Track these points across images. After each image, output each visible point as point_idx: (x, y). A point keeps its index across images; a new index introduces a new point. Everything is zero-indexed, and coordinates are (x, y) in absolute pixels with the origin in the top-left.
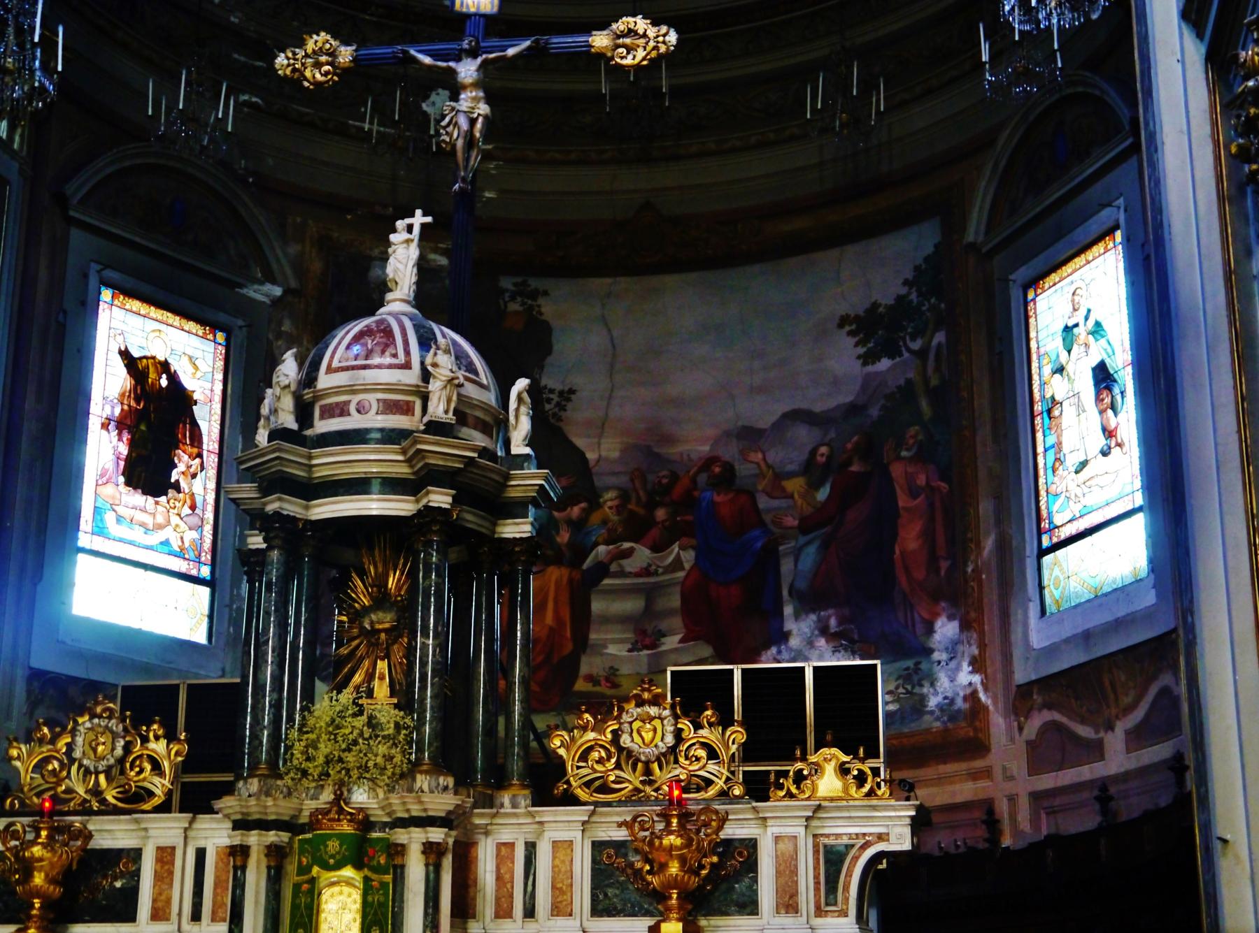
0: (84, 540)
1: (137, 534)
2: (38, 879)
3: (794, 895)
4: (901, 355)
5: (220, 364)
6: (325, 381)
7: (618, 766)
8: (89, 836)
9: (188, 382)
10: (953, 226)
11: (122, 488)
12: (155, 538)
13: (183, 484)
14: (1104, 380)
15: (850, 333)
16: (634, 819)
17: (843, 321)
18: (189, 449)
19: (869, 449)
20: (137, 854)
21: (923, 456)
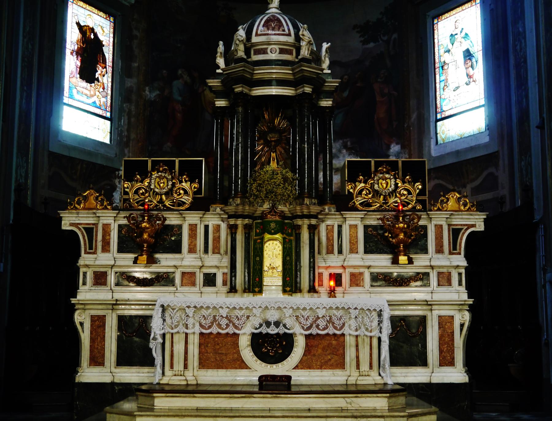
0: (66, 100)
1: (84, 99)
2: (145, 236)
3: (442, 246)
4: (379, 42)
5: (112, 30)
6: (255, 39)
7: (373, 196)
8: (165, 219)
9: (101, 37)
11: (79, 80)
12: (91, 101)
13: (100, 79)
14: (468, 56)
15: (357, 32)
16: (384, 217)
17: (355, 27)
18: (102, 65)
20: (180, 227)
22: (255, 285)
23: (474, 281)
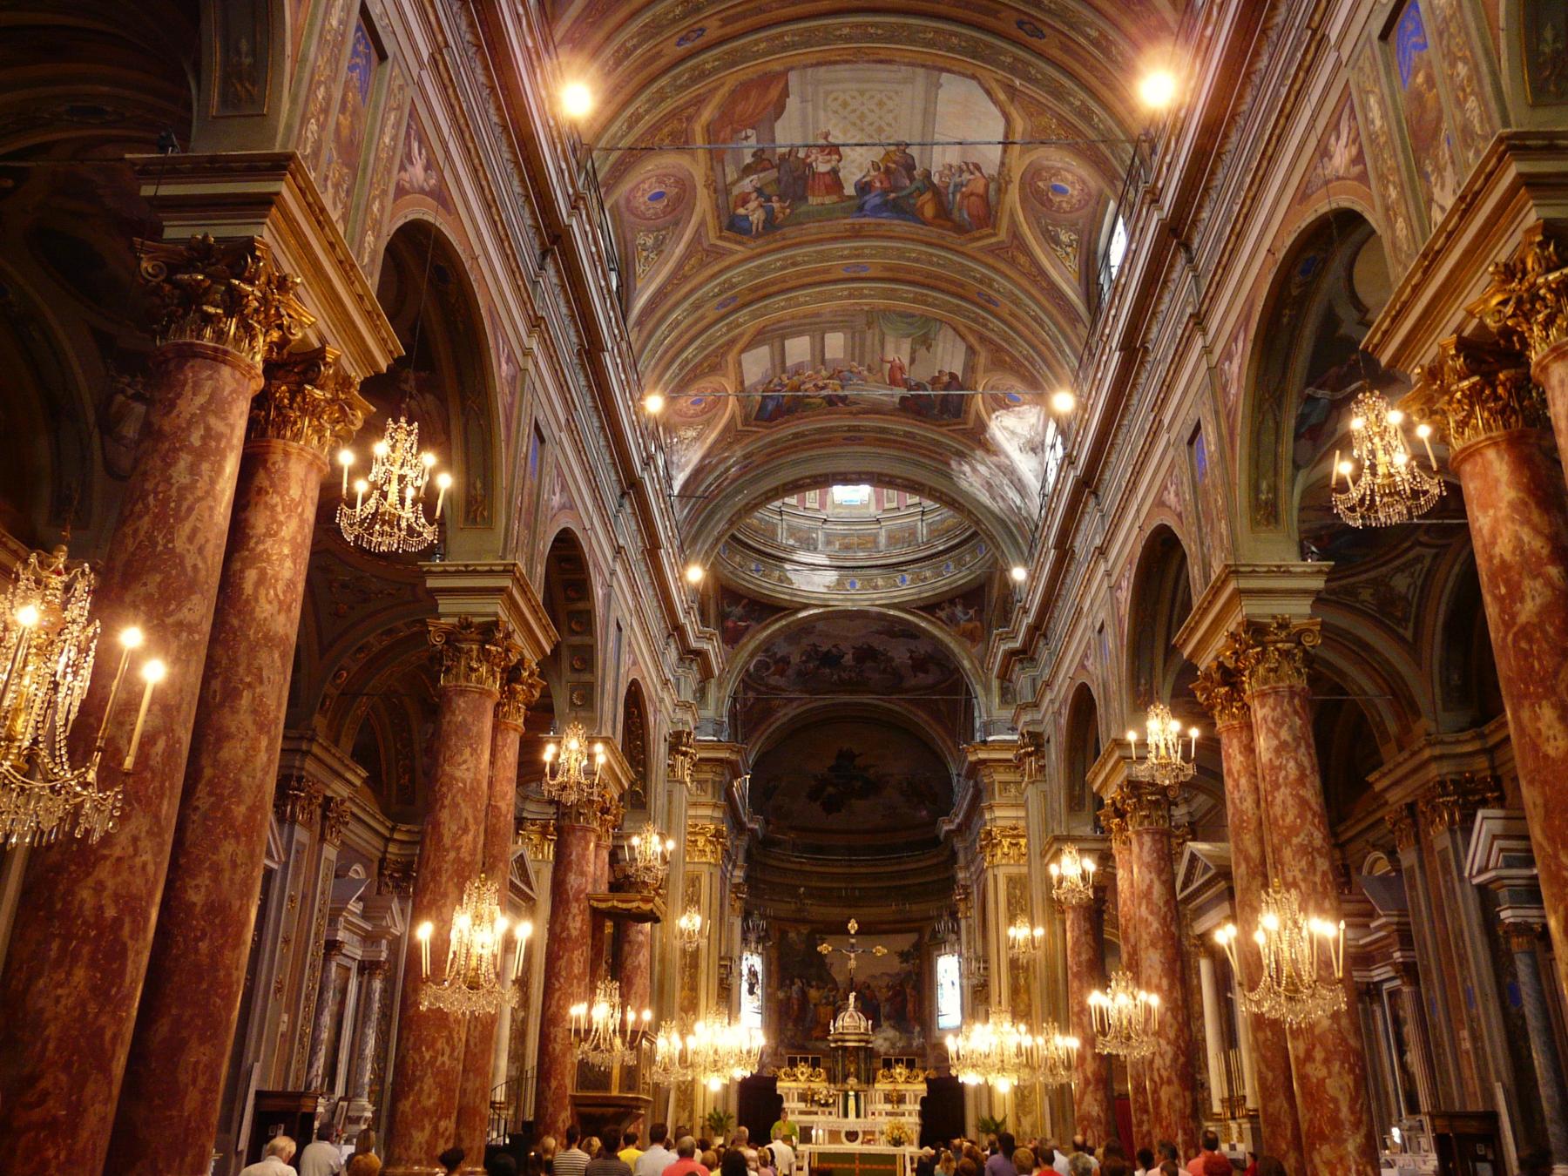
10: (921, 937)
19: (901, 985)
22: (846, 1115)
23: (922, 1114)
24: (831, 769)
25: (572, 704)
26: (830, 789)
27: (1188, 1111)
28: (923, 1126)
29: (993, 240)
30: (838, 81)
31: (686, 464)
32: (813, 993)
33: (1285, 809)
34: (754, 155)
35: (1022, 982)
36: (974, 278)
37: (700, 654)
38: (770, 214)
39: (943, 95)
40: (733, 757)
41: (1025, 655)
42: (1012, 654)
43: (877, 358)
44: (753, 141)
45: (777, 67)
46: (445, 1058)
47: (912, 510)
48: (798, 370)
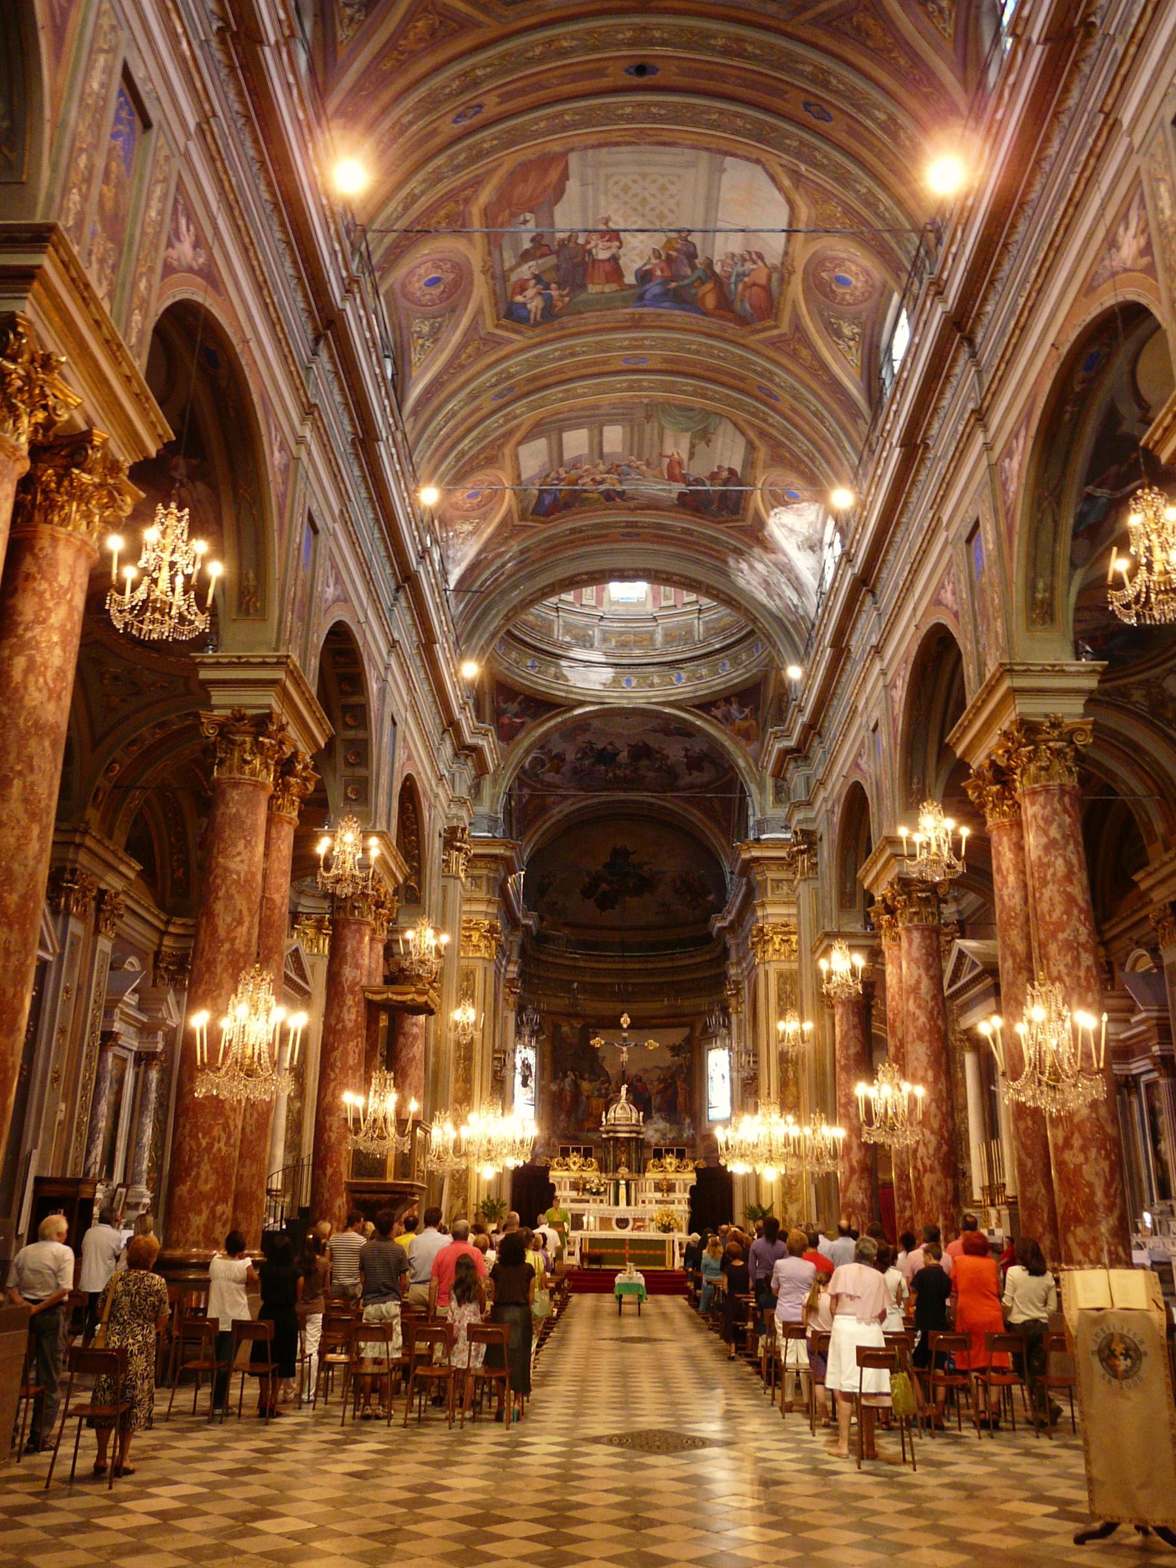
10: (692, 1031)
19: (672, 1077)
21: (685, 1081)
22: (617, 1203)
23: (691, 1202)
24: (606, 865)
25: (347, 799)
26: (604, 886)
27: (950, 1197)
28: (691, 1213)
29: (776, 332)
30: (619, 164)
31: (462, 559)
32: (585, 1085)
33: (1052, 905)
34: (533, 240)
35: (791, 1075)
36: (754, 371)
37: (475, 749)
38: (548, 301)
39: (726, 179)
40: (508, 853)
41: (800, 753)
42: (787, 752)
43: (655, 454)
44: (531, 225)
45: (557, 148)
46: (222, 1144)
47: (689, 608)
48: (576, 464)
